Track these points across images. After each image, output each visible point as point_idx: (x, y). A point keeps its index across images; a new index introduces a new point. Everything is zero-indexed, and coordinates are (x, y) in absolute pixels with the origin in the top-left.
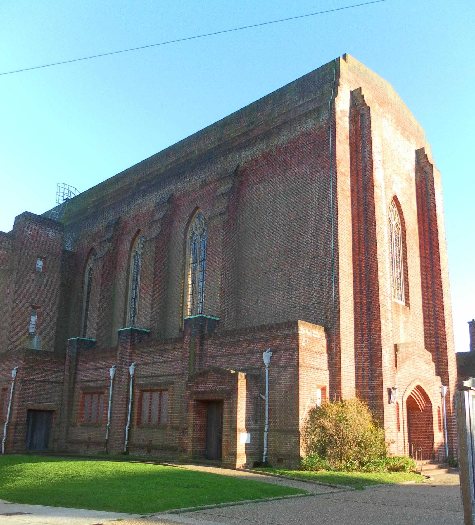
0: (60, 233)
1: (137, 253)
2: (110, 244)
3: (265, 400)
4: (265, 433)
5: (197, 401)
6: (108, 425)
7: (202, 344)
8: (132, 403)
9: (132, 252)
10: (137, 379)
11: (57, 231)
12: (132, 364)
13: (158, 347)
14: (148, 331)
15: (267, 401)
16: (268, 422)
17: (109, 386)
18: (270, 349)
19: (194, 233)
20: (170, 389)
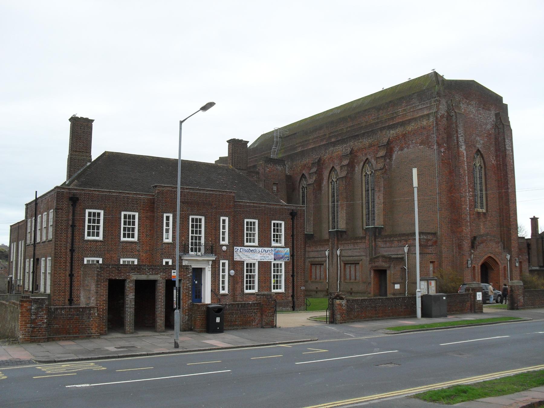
0: (283, 167)
1: (332, 180)
2: (316, 175)
3: (406, 269)
4: (406, 284)
5: (375, 271)
6: (327, 281)
7: (375, 241)
8: (340, 269)
9: (330, 179)
10: (342, 258)
11: (281, 166)
12: (339, 250)
13: (352, 241)
14: (345, 230)
15: (407, 269)
16: (408, 279)
17: (326, 261)
18: (407, 245)
19: (366, 173)
20: (360, 263)
